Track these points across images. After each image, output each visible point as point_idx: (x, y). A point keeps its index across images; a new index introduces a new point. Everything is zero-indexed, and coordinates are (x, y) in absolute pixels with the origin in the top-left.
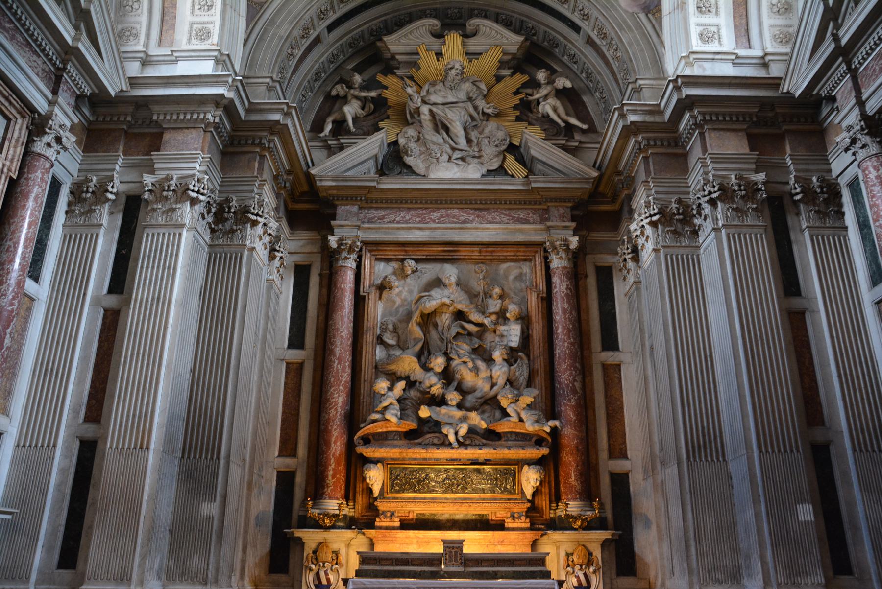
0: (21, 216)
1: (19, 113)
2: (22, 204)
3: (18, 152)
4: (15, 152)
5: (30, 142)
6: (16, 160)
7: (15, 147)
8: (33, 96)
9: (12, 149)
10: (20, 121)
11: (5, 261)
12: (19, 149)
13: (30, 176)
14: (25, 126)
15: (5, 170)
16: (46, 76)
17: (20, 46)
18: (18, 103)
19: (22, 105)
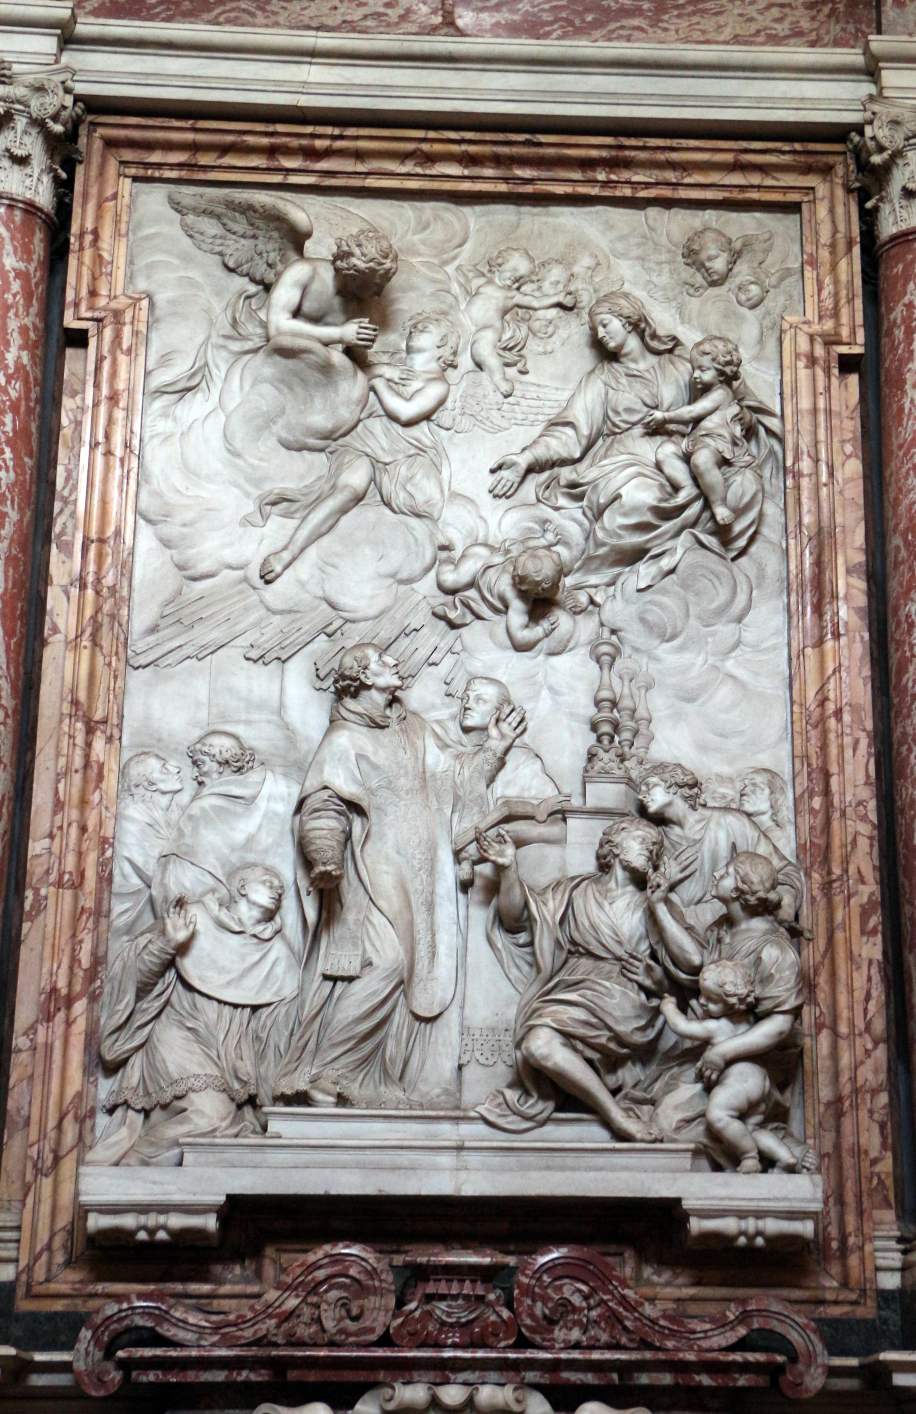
0: (900, 447)
1: (807, 170)
2: (895, 406)
3: (843, 277)
4: (836, 282)
5: (869, 219)
6: (843, 301)
7: (834, 267)
8: (814, 104)
9: (827, 280)
10: (822, 189)
11: (898, 598)
12: (843, 264)
13: (892, 317)
14: (840, 193)
15: (819, 351)
16: (833, 11)
17: (694, 13)
18: (784, 153)
19: (798, 146)
